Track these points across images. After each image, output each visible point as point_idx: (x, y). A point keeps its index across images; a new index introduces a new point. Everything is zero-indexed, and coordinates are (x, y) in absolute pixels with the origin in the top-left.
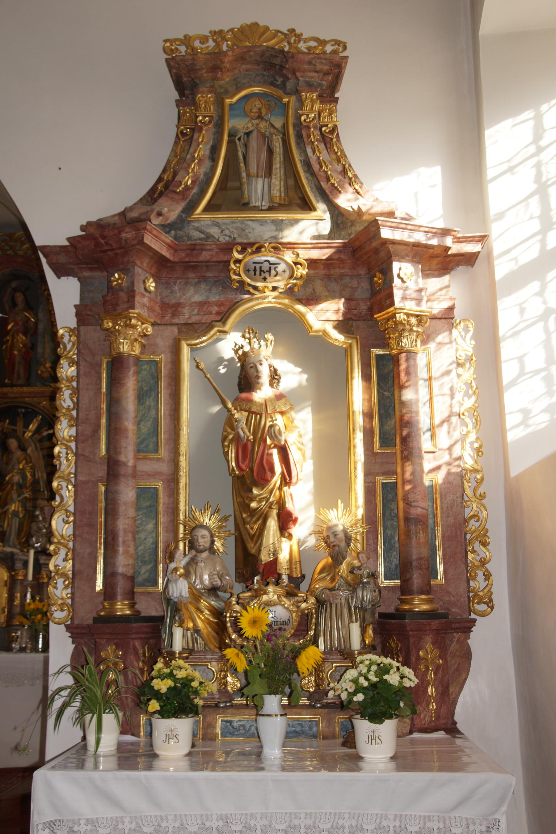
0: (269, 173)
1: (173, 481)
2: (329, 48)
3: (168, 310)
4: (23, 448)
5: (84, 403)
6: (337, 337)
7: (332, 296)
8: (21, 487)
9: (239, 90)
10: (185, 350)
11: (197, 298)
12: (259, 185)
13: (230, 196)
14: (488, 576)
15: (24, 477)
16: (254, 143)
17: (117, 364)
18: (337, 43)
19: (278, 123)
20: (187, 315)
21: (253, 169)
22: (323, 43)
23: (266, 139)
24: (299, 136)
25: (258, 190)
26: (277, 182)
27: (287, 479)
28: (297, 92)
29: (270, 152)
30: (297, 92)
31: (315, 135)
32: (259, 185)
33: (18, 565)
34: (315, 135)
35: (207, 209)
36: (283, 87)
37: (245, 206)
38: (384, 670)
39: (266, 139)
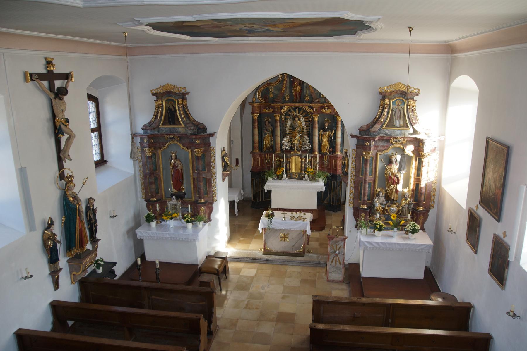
0: (400, 119)
1: (374, 181)
2: (416, 91)
3: (376, 146)
4: (299, 120)
5: (357, 165)
6: (411, 155)
7: (410, 144)
8: (299, 131)
9: (395, 98)
10: (379, 156)
11: (382, 144)
12: (398, 121)
13: (391, 124)
14: (434, 202)
15: (300, 129)
16: (397, 111)
17: (367, 160)
18: (418, 90)
19: (403, 107)
20: (379, 148)
21: (396, 118)
22: (415, 89)
23: (400, 110)
24: (407, 110)
25: (397, 123)
26: (401, 121)
27: (398, 182)
28: (407, 99)
29: (401, 114)
30: (407, 99)
31: (411, 110)
32: (398, 121)
33: (303, 157)
34: (411, 110)
35: (386, 126)
36: (404, 98)
37: (394, 126)
38: (415, 226)
39: (400, 110)
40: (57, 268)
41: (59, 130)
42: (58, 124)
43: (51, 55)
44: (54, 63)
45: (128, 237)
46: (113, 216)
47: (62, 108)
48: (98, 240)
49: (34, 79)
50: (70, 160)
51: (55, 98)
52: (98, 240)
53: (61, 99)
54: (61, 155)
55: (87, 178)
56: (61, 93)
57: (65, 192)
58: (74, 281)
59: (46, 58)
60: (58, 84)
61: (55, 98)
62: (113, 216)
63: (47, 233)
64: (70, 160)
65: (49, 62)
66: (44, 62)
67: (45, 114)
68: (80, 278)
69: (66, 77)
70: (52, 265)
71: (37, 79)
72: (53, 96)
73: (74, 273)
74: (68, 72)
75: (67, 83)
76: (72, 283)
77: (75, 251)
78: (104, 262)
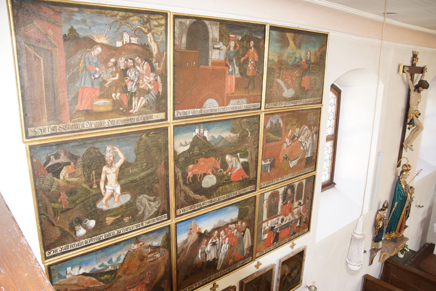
40: (378, 247)
41: (411, 121)
42: (411, 115)
43: (417, 49)
44: (418, 57)
45: (421, 227)
46: (419, 206)
47: (419, 101)
48: (406, 227)
49: (405, 71)
50: (412, 150)
51: (415, 91)
52: (406, 227)
53: (419, 92)
54: (404, 144)
55: (422, 170)
56: (423, 85)
57: (399, 179)
58: (382, 259)
59: (413, 52)
60: (417, 77)
61: (415, 91)
62: (419, 206)
63: (380, 215)
64: (412, 150)
65: (415, 56)
66: (411, 56)
67: (402, 105)
68: (386, 259)
69: (422, 70)
70: (375, 244)
71: (407, 71)
72: (414, 88)
73: (385, 253)
74: (422, 66)
75: (422, 76)
76: (379, 261)
77: (393, 235)
78: (410, 250)
